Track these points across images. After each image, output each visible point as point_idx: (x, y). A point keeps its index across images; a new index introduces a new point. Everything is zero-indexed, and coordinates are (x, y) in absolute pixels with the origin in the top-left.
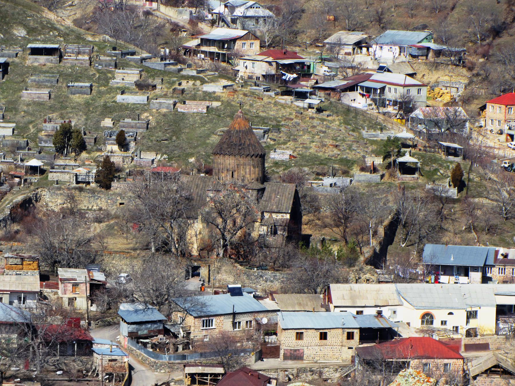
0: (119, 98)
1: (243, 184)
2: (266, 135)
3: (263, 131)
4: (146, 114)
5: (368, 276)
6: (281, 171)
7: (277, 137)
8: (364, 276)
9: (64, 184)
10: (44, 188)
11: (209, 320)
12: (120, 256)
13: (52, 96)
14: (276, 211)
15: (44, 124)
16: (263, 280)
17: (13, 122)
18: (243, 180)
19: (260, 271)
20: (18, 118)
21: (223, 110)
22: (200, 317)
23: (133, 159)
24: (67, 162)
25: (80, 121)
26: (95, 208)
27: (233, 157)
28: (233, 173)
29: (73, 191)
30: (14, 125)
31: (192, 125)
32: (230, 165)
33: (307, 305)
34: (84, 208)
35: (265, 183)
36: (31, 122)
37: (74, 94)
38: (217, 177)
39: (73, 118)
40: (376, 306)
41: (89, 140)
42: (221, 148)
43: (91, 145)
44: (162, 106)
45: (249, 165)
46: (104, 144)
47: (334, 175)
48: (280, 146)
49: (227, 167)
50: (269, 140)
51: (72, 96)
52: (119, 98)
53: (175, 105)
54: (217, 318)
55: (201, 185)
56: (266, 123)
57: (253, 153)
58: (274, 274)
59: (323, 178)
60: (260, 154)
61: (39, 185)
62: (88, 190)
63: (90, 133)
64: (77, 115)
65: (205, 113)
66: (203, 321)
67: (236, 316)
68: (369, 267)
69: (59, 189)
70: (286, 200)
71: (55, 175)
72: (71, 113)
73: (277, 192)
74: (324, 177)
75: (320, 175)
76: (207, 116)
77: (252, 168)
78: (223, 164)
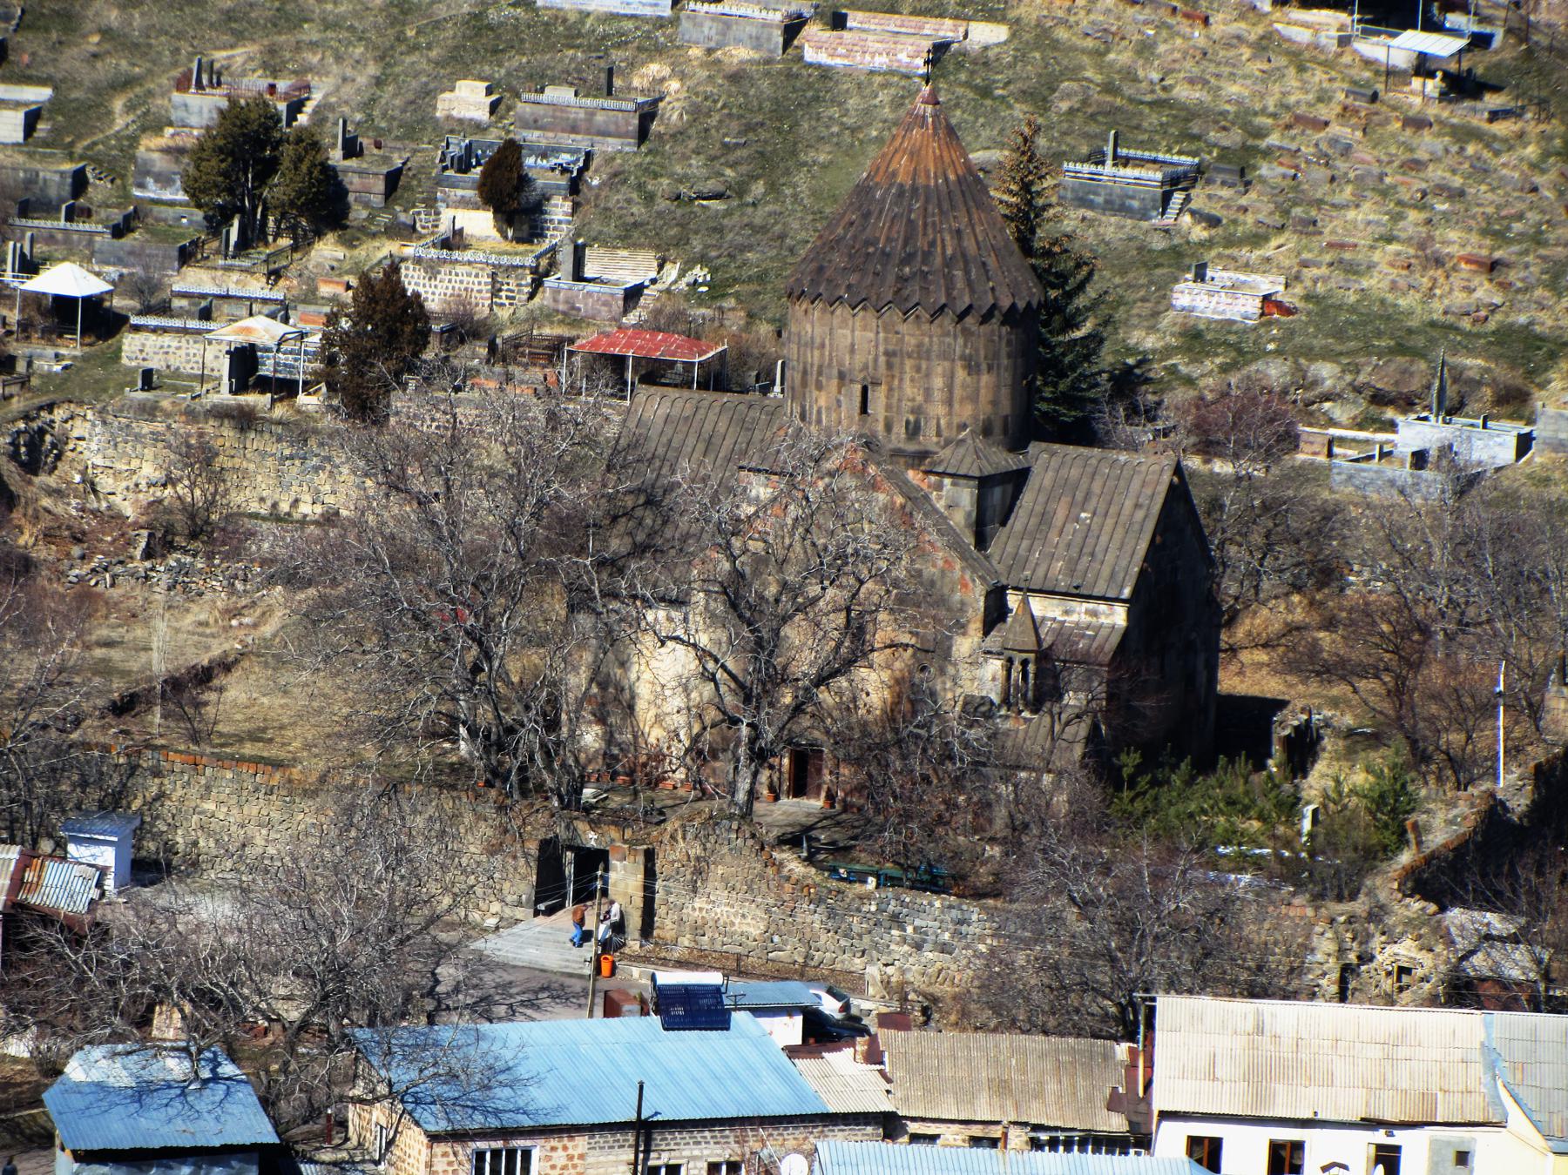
1: (912, 447)
2: (1178, 197)
3: (1159, 176)
4: (655, 69)
5: (1406, 950)
6: (1207, 374)
7: (1228, 207)
8: (1390, 949)
9: (176, 389)
10: (80, 403)
11: (511, 1153)
12: (238, 778)
14: (1062, 586)
15: (177, 96)
16: (904, 940)
17: (41, 82)
18: (914, 431)
19: (890, 893)
20: (71, 60)
21: (1011, 66)
22: (457, 1136)
23: (537, 284)
24: (233, 283)
25: (348, 90)
26: (305, 508)
27: (870, 316)
28: (865, 390)
29: (210, 427)
30: (39, 94)
31: (854, 130)
32: (852, 350)
33: (1039, 1094)
34: (254, 507)
35: (1034, 448)
36: (127, 83)
38: (797, 409)
39: (320, 71)
40: (1370, 1124)
41: (362, 182)
42: (821, 269)
43: (367, 205)
45: (945, 355)
46: (431, 203)
47: (1451, 410)
49: (841, 364)
53: (793, 29)
54: (554, 1142)
55: (729, 442)
56: (1198, 138)
57: (967, 301)
58: (955, 913)
59: (1400, 419)
60: (1006, 303)
62: (279, 423)
63: (378, 146)
64: (339, 59)
66: (480, 1156)
67: (657, 1137)
68: (1416, 905)
69: (149, 411)
70: (1120, 531)
71: (152, 340)
72: (313, 45)
73: (1079, 496)
74: (1405, 412)
75: (1383, 404)
77: (961, 374)
78: (823, 346)
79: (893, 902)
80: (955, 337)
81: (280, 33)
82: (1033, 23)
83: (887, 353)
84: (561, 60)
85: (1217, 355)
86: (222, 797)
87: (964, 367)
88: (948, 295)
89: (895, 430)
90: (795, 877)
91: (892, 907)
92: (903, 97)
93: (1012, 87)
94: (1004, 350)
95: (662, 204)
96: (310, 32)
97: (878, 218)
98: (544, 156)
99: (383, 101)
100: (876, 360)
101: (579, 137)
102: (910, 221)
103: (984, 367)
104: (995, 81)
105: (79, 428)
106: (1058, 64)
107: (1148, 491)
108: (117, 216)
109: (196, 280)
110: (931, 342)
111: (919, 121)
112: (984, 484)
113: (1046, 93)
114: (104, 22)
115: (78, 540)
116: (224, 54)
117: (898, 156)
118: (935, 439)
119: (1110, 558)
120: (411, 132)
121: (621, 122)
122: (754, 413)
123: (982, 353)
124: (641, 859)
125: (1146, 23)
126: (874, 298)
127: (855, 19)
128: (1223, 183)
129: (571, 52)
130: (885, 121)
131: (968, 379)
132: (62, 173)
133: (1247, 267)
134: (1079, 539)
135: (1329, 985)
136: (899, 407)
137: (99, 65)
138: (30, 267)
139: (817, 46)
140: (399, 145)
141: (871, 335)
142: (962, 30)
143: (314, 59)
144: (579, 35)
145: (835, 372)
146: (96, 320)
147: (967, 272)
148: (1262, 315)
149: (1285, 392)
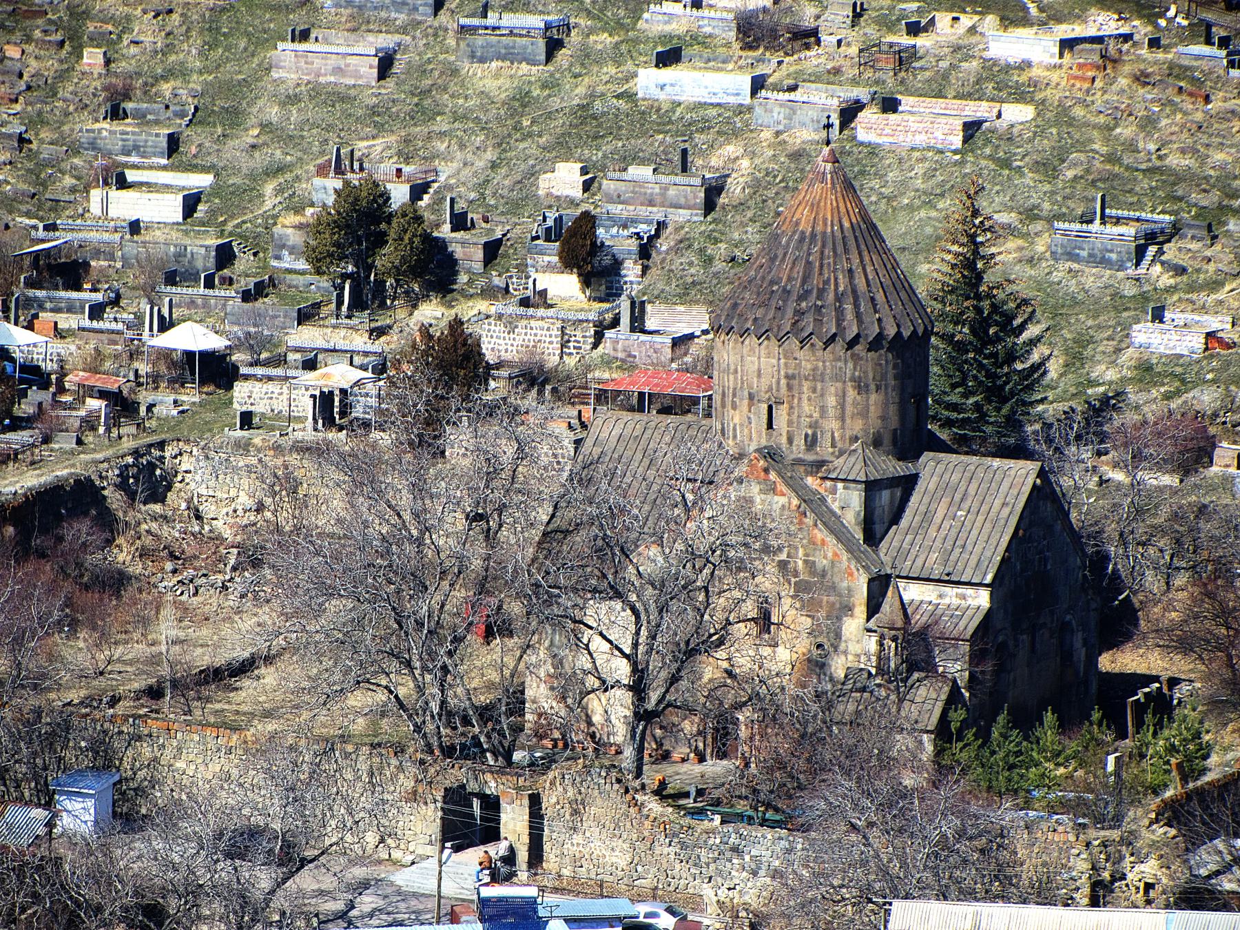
0: (651, 82)
1: (810, 457)
2: (1152, 250)
3: (1133, 231)
4: (731, 149)
7: (1194, 258)
10: (188, 441)
13: (397, 68)
15: (318, 181)
17: (205, 169)
18: (811, 442)
19: (730, 828)
20: (234, 150)
21: (1031, 140)
23: (599, 337)
24: (339, 338)
25: (467, 172)
28: (770, 408)
29: (293, 459)
30: (202, 180)
31: (889, 199)
32: (759, 376)
36: (281, 169)
37: (482, 60)
39: (447, 157)
41: (466, 250)
42: (735, 305)
43: (468, 271)
44: (796, 118)
45: (836, 378)
46: (522, 268)
48: (1194, 296)
50: (1158, 268)
51: (466, 67)
52: (651, 82)
53: (849, 113)
56: (1181, 199)
57: (855, 330)
60: (891, 331)
61: (187, 427)
63: (486, 220)
64: (462, 146)
65: (955, 152)
69: (243, 447)
70: (988, 525)
71: (257, 388)
72: (442, 134)
73: (958, 497)
76: (956, 163)
77: (851, 393)
78: (736, 371)
79: (733, 836)
80: (846, 362)
81: (415, 125)
82: (1056, 103)
83: (787, 377)
84: (652, 144)
85: (1163, 385)
86: (191, 757)
87: (854, 388)
88: (838, 325)
89: (795, 443)
90: (653, 815)
91: (733, 840)
92: (936, 170)
93: (1027, 159)
94: (891, 373)
95: (719, 265)
96: (441, 124)
97: (783, 260)
98: (625, 226)
99: (495, 182)
100: (778, 383)
101: (655, 209)
102: (808, 263)
103: (873, 387)
104: (1015, 154)
105: (186, 463)
106: (1071, 138)
107: (1014, 492)
108: (251, 283)
109: (308, 336)
110: (824, 366)
111: (820, 177)
112: (871, 487)
113: (1056, 163)
114: (265, 118)
115: (173, 556)
116: (365, 143)
117: (801, 208)
118: (831, 450)
119: (978, 549)
120: (515, 207)
121: (690, 196)
122: (692, 432)
123: (871, 375)
124: (526, 802)
125: (1153, 101)
126: (775, 330)
127: (907, 102)
128: (1193, 238)
129: (661, 136)
130: (917, 190)
131: (858, 398)
132: (207, 247)
133: (1203, 309)
134: (954, 532)
135: (1083, 896)
136: (799, 422)
137: (257, 154)
138: (165, 325)
139: (871, 127)
140: (503, 219)
141: (774, 361)
142: (995, 111)
143: (442, 146)
144: (670, 122)
145: (746, 393)
146: (215, 371)
147: (856, 305)
148: (1206, 349)
149: (1215, 415)
